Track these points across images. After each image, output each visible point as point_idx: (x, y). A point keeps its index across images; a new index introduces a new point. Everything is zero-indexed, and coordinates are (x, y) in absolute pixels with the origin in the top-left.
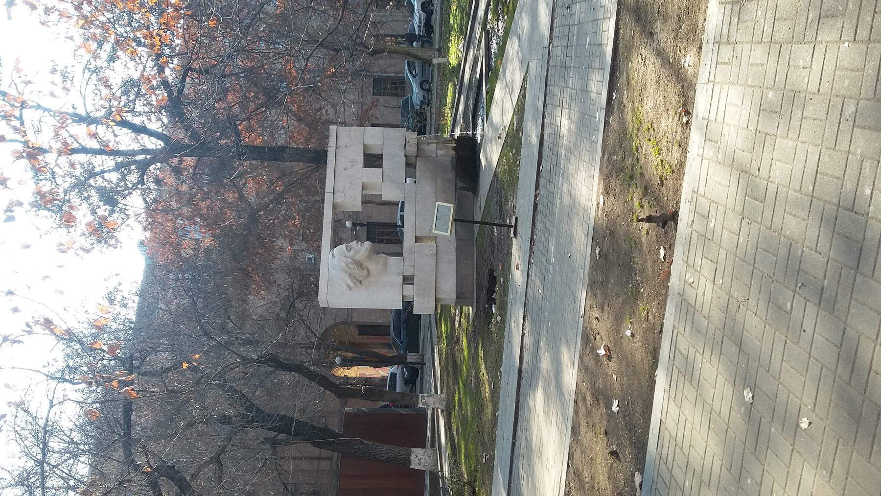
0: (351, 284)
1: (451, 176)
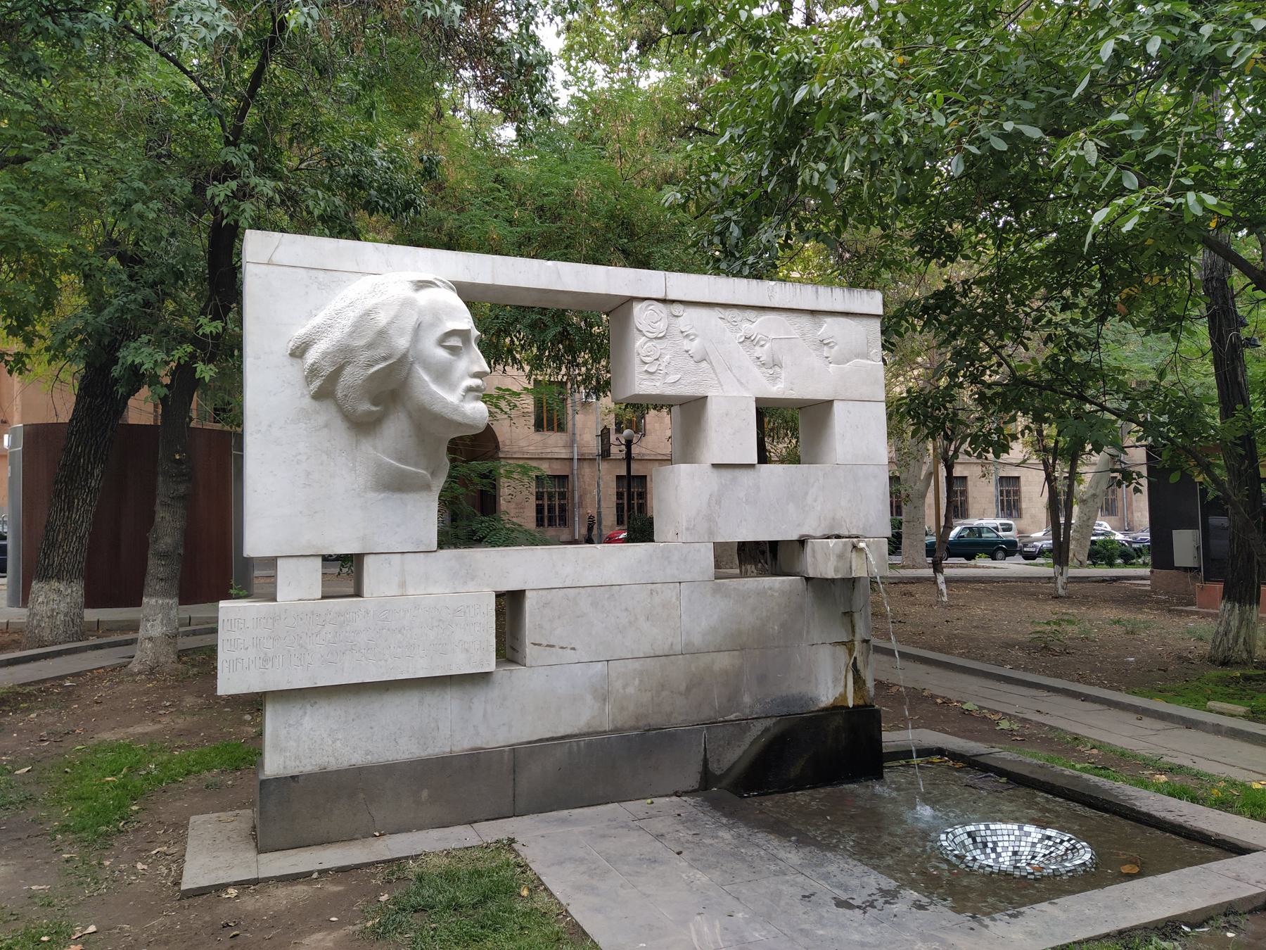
0: (312, 356)
1: (747, 699)
